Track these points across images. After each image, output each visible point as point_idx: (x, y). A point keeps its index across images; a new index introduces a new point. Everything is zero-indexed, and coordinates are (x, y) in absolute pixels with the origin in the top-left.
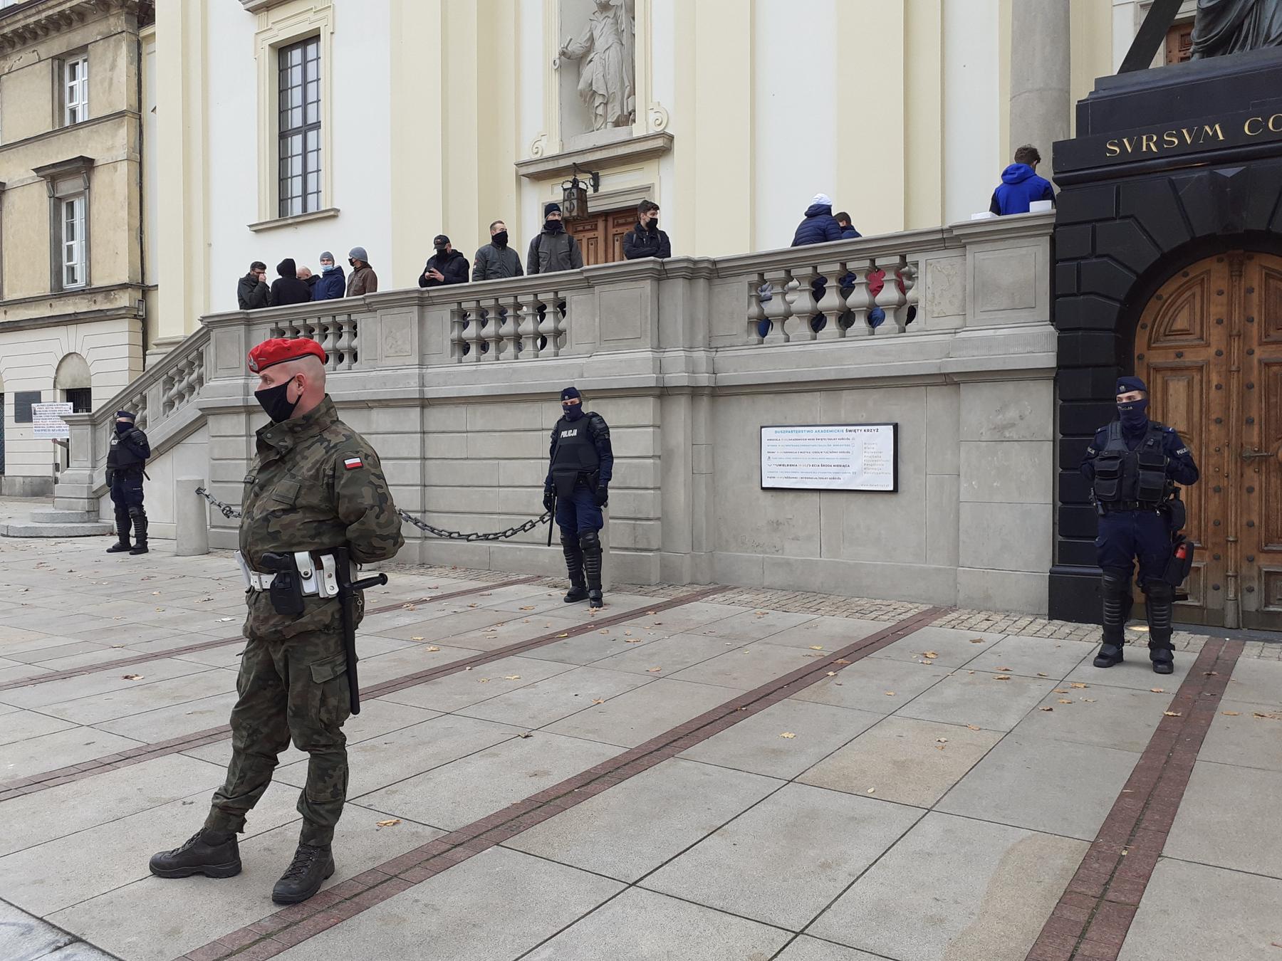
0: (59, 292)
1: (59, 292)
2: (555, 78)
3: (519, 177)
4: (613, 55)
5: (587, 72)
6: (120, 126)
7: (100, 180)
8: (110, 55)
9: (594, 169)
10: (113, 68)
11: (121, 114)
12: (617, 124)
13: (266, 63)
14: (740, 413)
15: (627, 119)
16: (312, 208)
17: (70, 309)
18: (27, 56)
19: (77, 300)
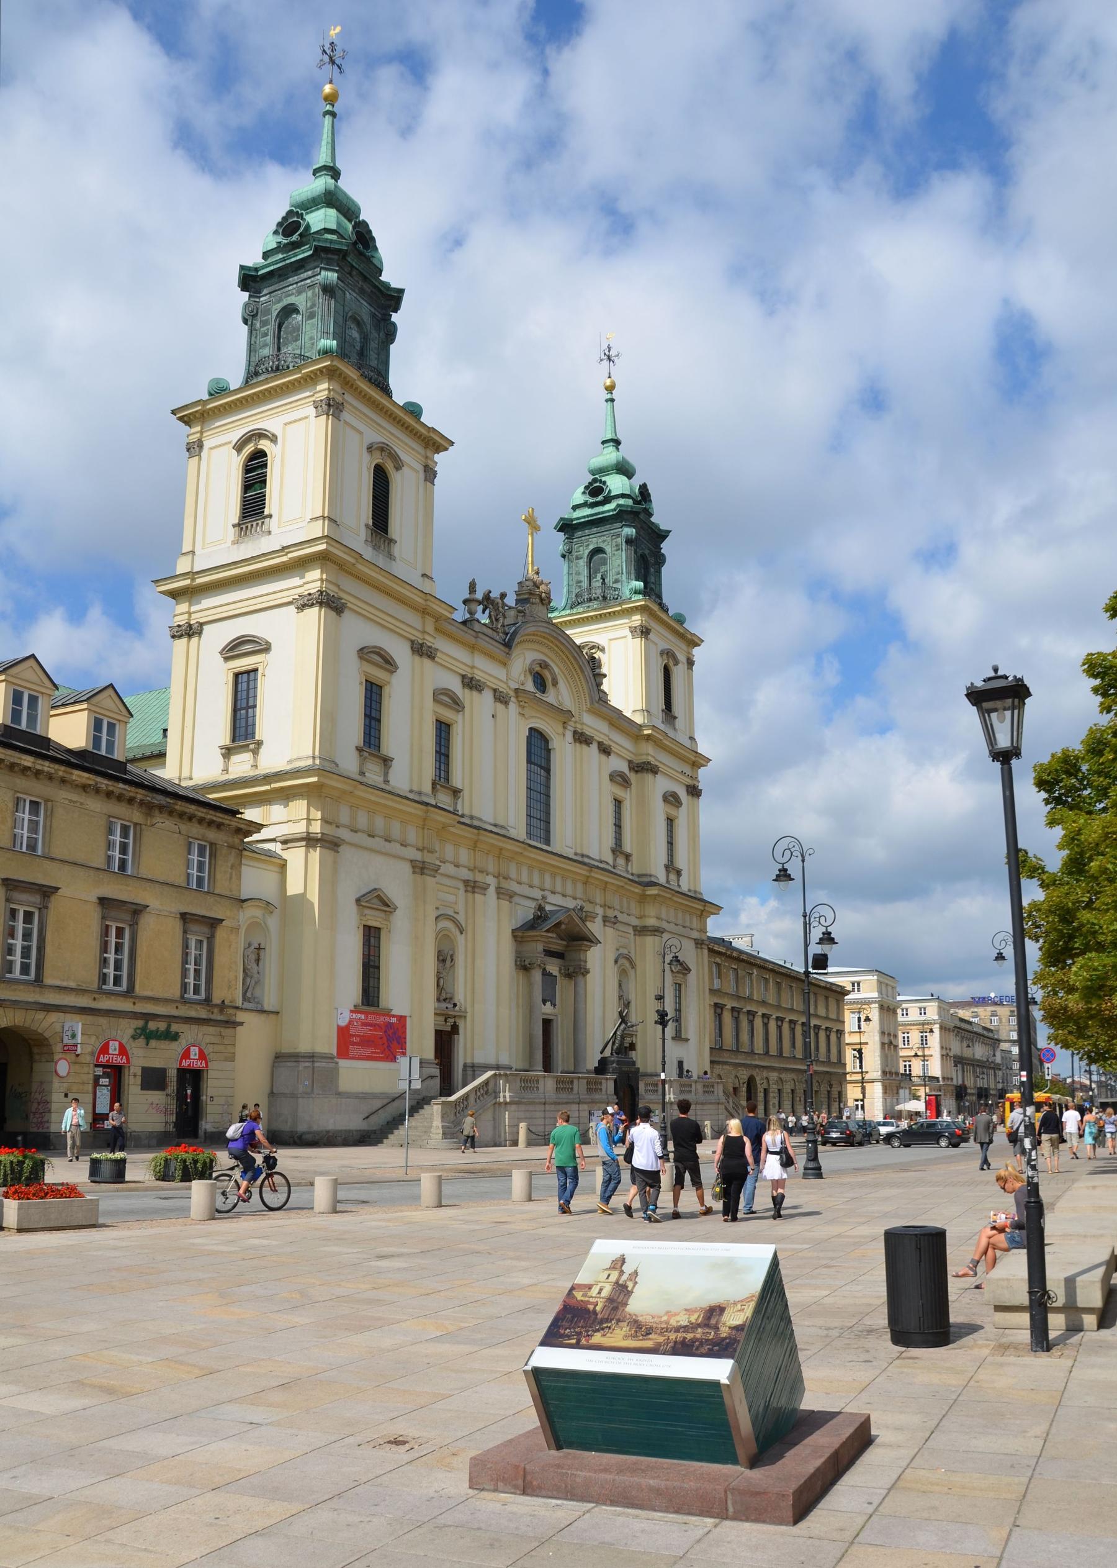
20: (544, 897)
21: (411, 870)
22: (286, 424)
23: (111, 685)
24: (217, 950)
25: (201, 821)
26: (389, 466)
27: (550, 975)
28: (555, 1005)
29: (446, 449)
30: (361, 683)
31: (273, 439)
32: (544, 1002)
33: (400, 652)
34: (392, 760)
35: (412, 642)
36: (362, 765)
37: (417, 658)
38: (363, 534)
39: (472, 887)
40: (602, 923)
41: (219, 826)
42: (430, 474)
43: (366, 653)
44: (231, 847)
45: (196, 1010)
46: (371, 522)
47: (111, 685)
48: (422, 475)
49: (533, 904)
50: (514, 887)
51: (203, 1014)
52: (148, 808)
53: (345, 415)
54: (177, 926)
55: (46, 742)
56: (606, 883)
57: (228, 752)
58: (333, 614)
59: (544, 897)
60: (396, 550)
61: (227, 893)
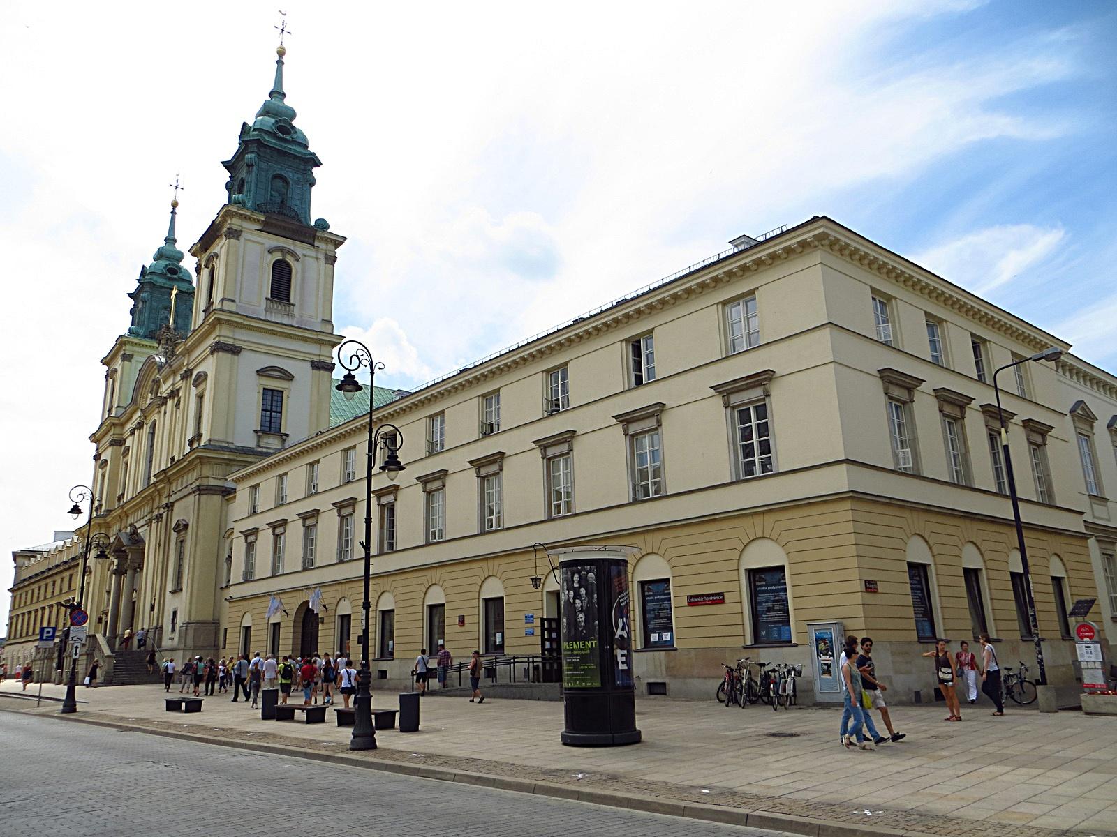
22: (221, 248)
26: (289, 259)
29: (341, 243)
30: (259, 392)
31: (217, 256)
33: (301, 370)
34: (287, 435)
35: (312, 362)
36: (259, 441)
37: (316, 372)
38: (264, 304)
42: (332, 260)
46: (269, 296)
48: (323, 261)
53: (244, 235)
57: (191, 442)
58: (229, 355)
60: (296, 311)
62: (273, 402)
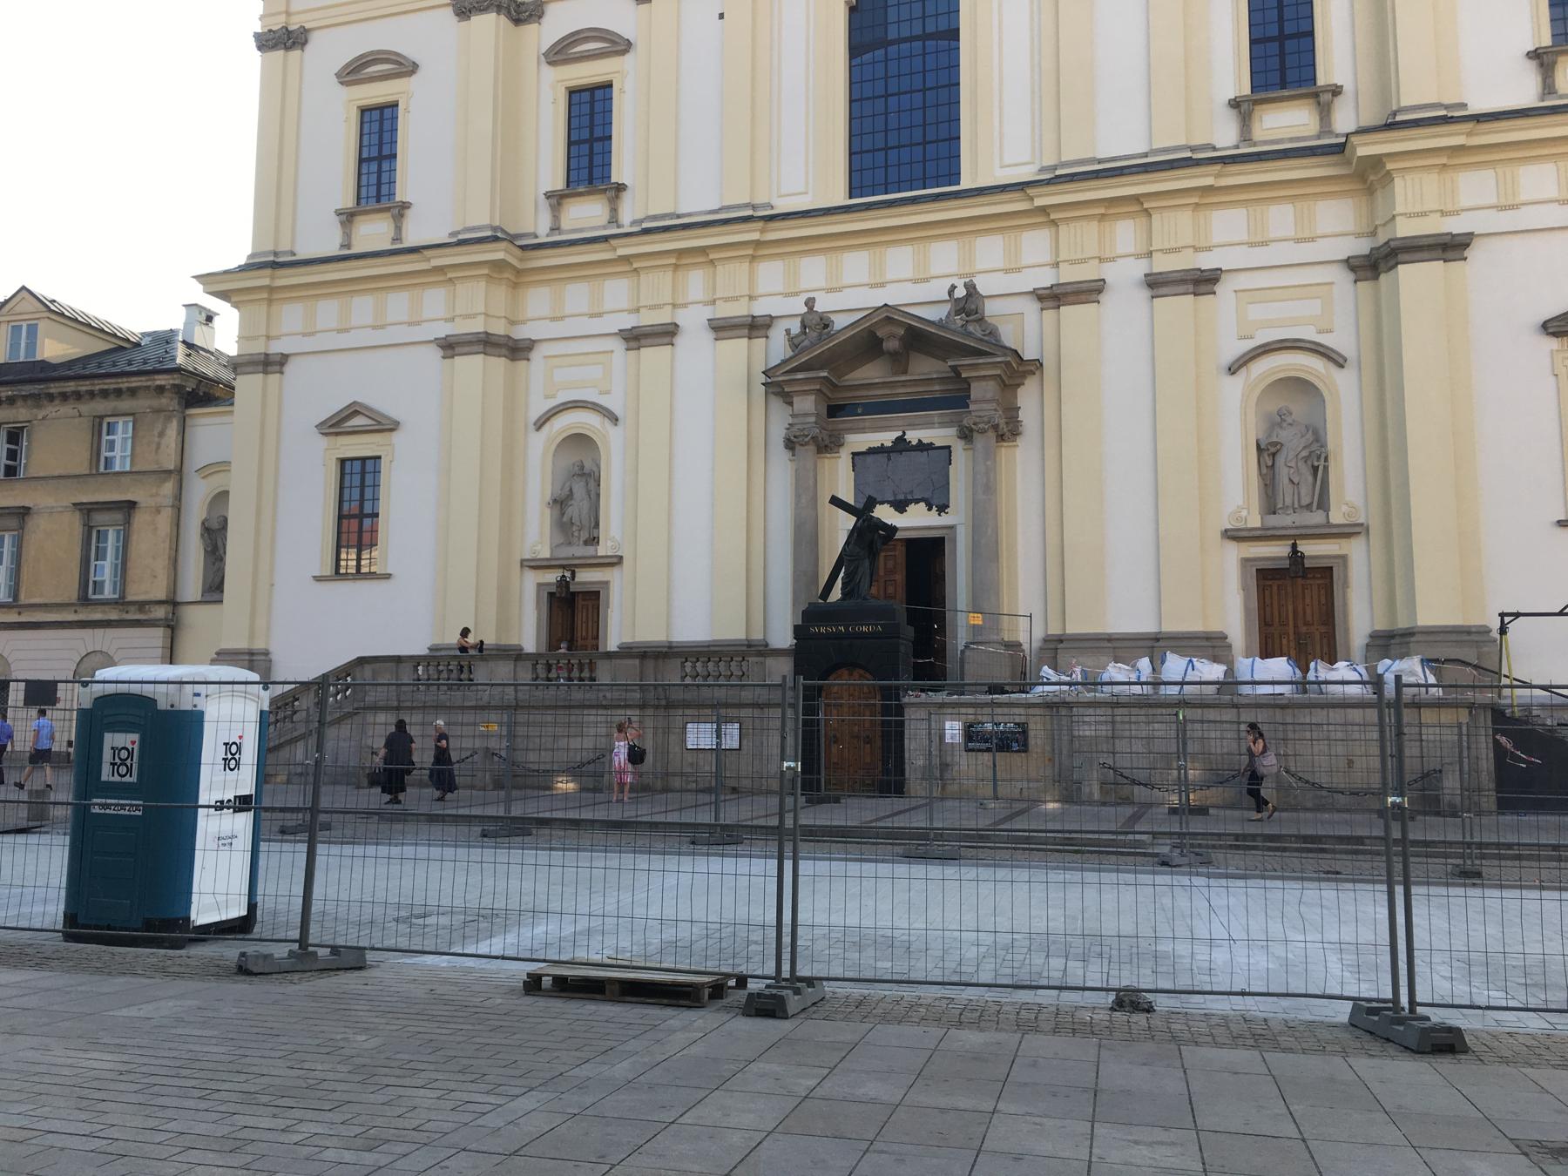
0: (84, 601)
1: (84, 601)
2: (548, 512)
3: (522, 566)
4: (585, 505)
5: (569, 511)
6: (164, 481)
7: (140, 519)
8: (159, 427)
9: (572, 569)
10: (161, 434)
11: (170, 472)
12: (586, 543)
13: (334, 469)
14: (677, 716)
15: (594, 541)
16: (364, 570)
17: (97, 616)
18: (67, 409)
19: (106, 608)
20: (810, 303)
21: (440, 353)
23: (23, 288)
24: (134, 537)
25: (105, 394)
27: (922, 447)
28: (942, 509)
32: (900, 506)
39: (635, 338)
40: (1146, 293)
41: (133, 392)
43: (353, 73)
44: (158, 411)
45: (104, 612)
47: (23, 288)
49: (795, 327)
50: (760, 309)
51: (114, 616)
52: (36, 399)
54: (75, 522)
55: (44, 365)
56: (1137, 199)
59: (810, 303)
61: (154, 467)
62: (378, 136)
